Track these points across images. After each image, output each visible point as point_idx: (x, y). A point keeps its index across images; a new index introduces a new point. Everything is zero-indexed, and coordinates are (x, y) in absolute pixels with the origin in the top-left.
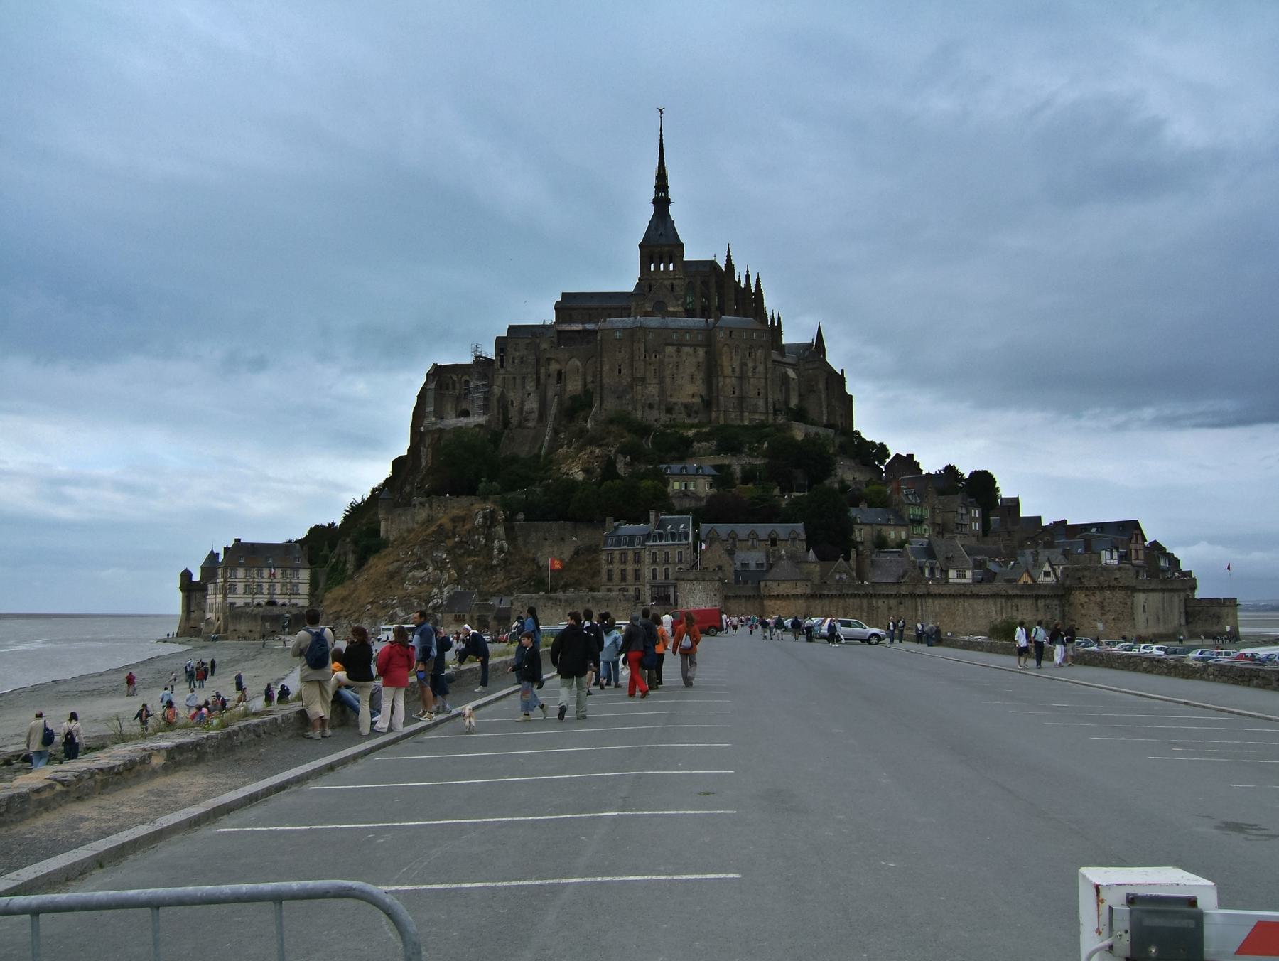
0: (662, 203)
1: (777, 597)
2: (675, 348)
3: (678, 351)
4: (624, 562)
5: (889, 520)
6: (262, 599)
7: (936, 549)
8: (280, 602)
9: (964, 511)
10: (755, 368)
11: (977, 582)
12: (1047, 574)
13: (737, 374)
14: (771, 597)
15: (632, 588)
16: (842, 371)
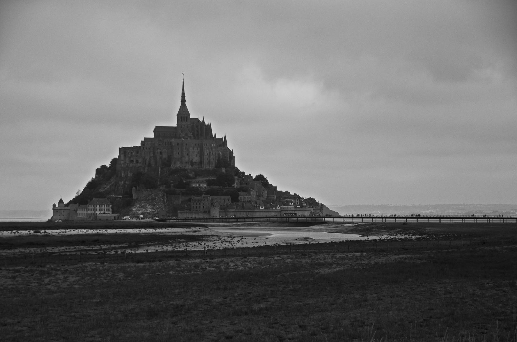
0: (183, 100)
1: (229, 212)
2: (192, 148)
3: (193, 149)
4: (197, 204)
5: (247, 195)
6: (102, 212)
7: (257, 202)
8: (106, 213)
9: (263, 192)
10: (212, 154)
11: (265, 209)
12: (278, 207)
13: (208, 155)
14: (228, 212)
15: (198, 210)
16: (232, 150)
